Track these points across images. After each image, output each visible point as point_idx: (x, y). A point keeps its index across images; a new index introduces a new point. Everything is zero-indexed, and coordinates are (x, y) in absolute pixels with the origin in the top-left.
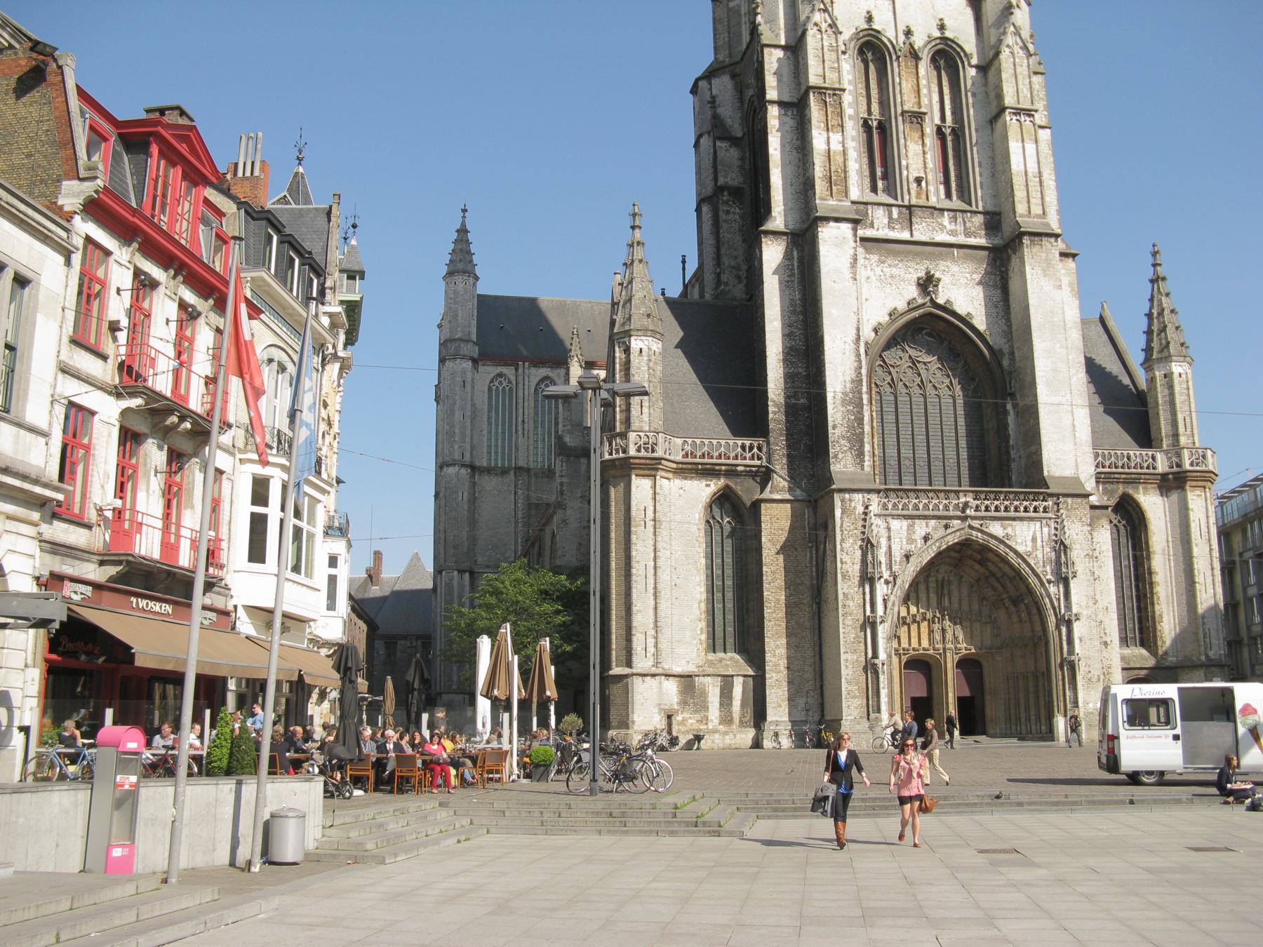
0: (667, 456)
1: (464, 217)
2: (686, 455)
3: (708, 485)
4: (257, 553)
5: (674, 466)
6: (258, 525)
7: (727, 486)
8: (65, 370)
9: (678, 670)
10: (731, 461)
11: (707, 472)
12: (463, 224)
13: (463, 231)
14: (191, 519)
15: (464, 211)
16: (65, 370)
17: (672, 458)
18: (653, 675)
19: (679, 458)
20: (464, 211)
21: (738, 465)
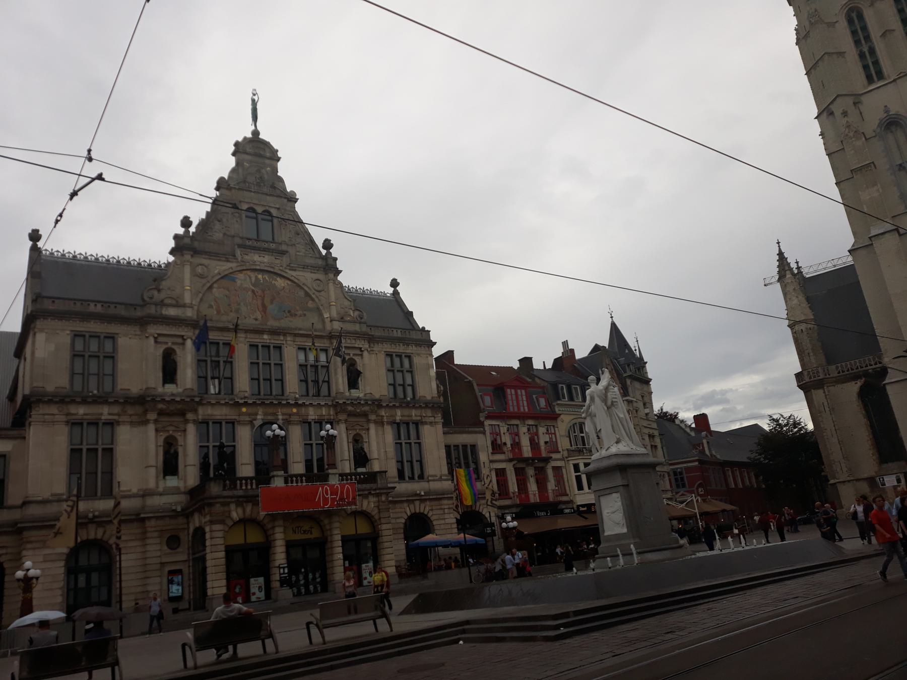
0: (828, 376)
1: (779, 246)
2: (839, 373)
3: (856, 383)
4: (580, 487)
5: (834, 379)
6: (578, 479)
7: (865, 382)
8: (491, 461)
9: (865, 476)
10: (865, 369)
11: (855, 377)
12: (780, 250)
13: (781, 254)
14: (551, 485)
15: (778, 243)
16: (491, 461)
17: (831, 376)
18: (849, 481)
19: (836, 374)
20: (778, 243)
21: (868, 370)
